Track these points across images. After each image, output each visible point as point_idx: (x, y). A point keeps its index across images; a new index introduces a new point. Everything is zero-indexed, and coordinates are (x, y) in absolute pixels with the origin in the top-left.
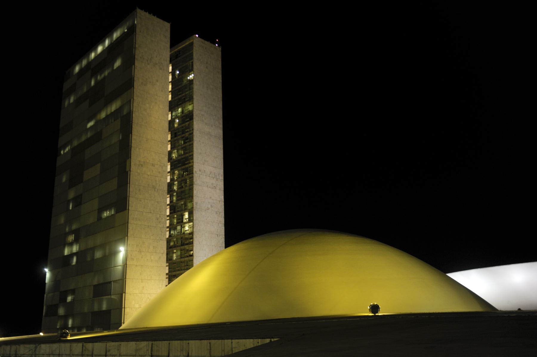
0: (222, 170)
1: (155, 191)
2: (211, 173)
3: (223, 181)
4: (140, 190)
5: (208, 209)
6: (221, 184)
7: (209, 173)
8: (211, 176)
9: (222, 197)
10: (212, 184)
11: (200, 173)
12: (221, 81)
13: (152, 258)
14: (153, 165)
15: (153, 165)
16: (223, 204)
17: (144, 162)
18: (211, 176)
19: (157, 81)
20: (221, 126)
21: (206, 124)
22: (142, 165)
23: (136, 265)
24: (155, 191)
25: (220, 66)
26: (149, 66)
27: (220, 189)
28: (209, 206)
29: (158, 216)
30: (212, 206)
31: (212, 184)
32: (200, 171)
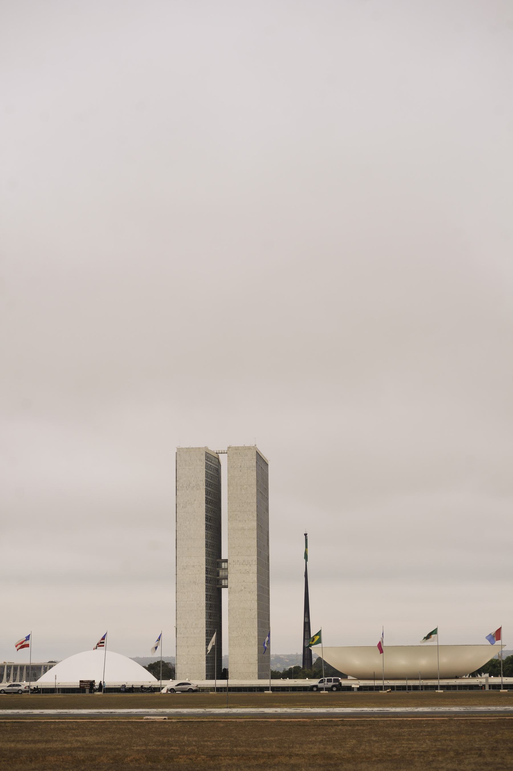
0: (256, 557)
3: (256, 565)
5: (242, 590)
6: (255, 568)
9: (256, 579)
10: (246, 570)
12: (256, 477)
14: (193, 566)
15: (193, 566)
16: (256, 584)
19: (195, 500)
20: (255, 518)
21: (240, 521)
25: (255, 464)
26: (187, 492)
27: (253, 573)
28: (243, 588)
29: (199, 602)
30: (245, 588)
31: (246, 570)
32: (234, 562)
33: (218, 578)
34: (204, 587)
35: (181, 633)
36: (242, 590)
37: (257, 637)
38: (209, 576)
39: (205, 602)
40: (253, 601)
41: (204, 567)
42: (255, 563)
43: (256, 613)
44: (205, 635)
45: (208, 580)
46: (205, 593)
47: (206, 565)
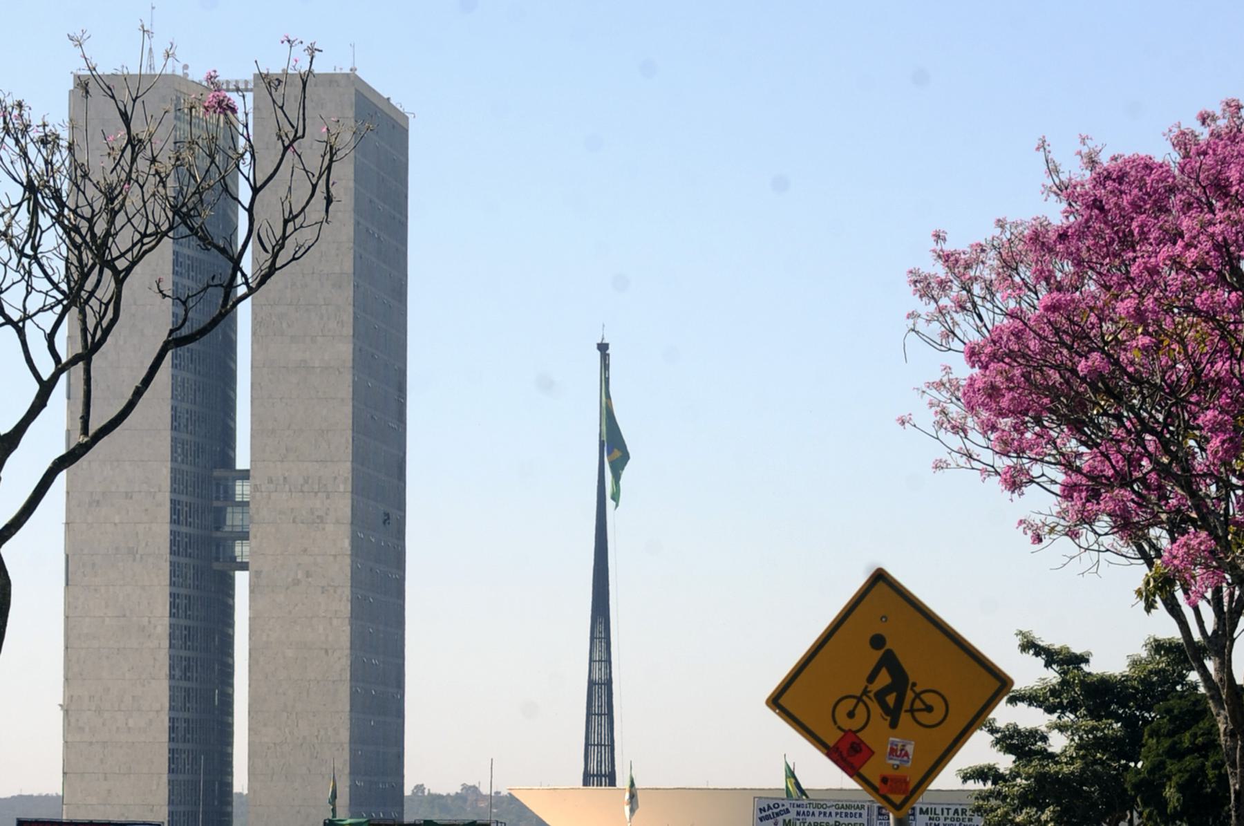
0: (349, 465)
1: (134, 560)
2: (306, 482)
3: (349, 495)
4: (94, 565)
5: (297, 582)
6: (343, 506)
7: (301, 481)
8: (306, 488)
9: (347, 544)
10: (312, 511)
11: (272, 486)
12: (352, 184)
13: (131, 723)
14: (128, 496)
15: (128, 496)
16: (348, 561)
17: (104, 493)
18: (306, 488)
22: (98, 502)
23: (91, 743)
24: (134, 560)
27: (337, 522)
30: (308, 575)
31: (312, 511)
32: (270, 481)
33: (219, 534)
34: (166, 568)
35: (81, 729)
36: (297, 582)
37: (347, 747)
38: (184, 529)
39: (166, 621)
40: (335, 622)
41: (165, 498)
42: (345, 487)
43: (346, 662)
44: (165, 737)
45: (177, 545)
46: (167, 591)
47: (173, 491)
